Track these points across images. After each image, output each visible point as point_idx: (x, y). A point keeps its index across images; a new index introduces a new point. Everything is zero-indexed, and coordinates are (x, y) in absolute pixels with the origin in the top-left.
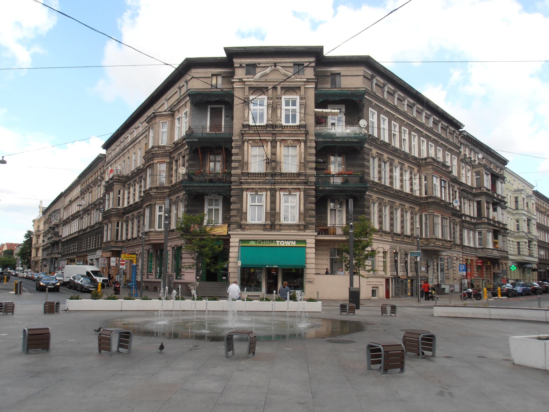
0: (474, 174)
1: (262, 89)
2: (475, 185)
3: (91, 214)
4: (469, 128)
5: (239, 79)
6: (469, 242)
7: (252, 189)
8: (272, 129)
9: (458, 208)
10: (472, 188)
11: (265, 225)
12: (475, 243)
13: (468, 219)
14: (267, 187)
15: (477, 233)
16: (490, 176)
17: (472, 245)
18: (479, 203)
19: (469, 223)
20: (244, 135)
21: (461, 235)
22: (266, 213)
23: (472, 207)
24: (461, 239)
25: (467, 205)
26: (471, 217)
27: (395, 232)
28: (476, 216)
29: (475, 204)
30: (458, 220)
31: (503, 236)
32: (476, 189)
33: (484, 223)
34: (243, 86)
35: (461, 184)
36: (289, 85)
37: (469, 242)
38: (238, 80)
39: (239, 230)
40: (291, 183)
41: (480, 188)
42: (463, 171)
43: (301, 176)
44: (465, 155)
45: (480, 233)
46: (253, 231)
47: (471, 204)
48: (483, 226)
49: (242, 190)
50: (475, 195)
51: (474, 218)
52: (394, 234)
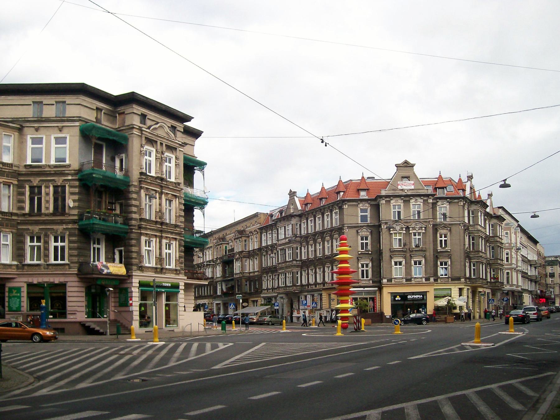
1: (153, 142)
5: (139, 127)
7: (147, 234)
8: (161, 182)
11: (156, 268)
14: (158, 234)
20: (163, 188)
22: (156, 257)
34: (140, 134)
36: (170, 144)
38: (138, 127)
39: (139, 272)
40: (172, 233)
43: (178, 228)
46: (148, 273)
49: (141, 234)
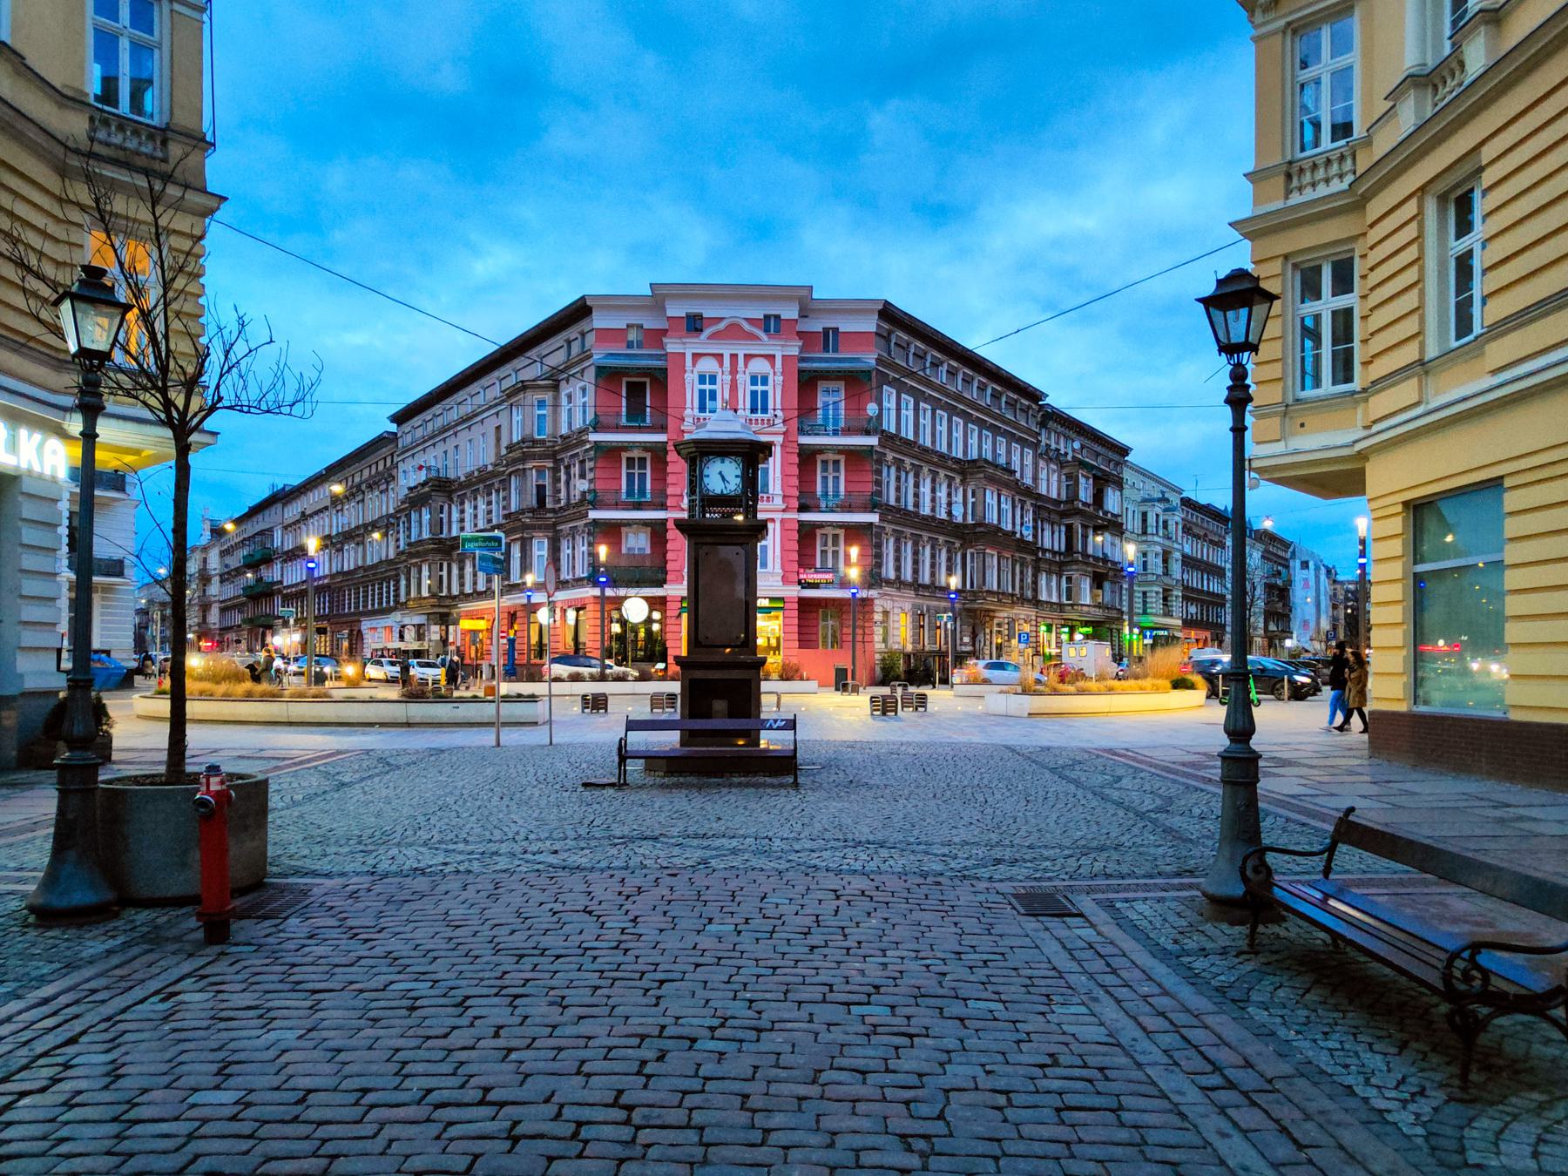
0: (1063, 477)
2: (1064, 497)
3: (363, 543)
4: (1057, 399)
6: (1050, 594)
9: (1030, 538)
10: (1057, 502)
12: (1060, 596)
13: (1048, 555)
15: (1064, 578)
16: (1091, 481)
17: (1055, 599)
18: (1069, 528)
19: (1050, 562)
21: (1035, 582)
23: (1056, 535)
24: (1035, 590)
25: (1047, 533)
26: (1054, 553)
27: (920, 581)
28: (1063, 548)
29: (1063, 529)
30: (1029, 558)
31: (1113, 582)
32: (1066, 502)
33: (1076, 562)
35: (1039, 497)
37: (1050, 594)
41: (1072, 502)
42: (1043, 475)
44: (1048, 446)
45: (1069, 580)
47: (1056, 528)
48: (1074, 567)
50: (1064, 515)
51: (1060, 554)
52: (920, 585)
